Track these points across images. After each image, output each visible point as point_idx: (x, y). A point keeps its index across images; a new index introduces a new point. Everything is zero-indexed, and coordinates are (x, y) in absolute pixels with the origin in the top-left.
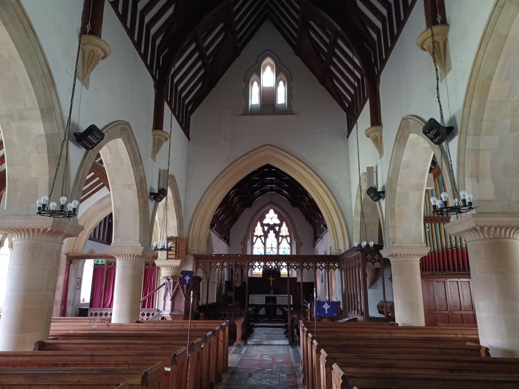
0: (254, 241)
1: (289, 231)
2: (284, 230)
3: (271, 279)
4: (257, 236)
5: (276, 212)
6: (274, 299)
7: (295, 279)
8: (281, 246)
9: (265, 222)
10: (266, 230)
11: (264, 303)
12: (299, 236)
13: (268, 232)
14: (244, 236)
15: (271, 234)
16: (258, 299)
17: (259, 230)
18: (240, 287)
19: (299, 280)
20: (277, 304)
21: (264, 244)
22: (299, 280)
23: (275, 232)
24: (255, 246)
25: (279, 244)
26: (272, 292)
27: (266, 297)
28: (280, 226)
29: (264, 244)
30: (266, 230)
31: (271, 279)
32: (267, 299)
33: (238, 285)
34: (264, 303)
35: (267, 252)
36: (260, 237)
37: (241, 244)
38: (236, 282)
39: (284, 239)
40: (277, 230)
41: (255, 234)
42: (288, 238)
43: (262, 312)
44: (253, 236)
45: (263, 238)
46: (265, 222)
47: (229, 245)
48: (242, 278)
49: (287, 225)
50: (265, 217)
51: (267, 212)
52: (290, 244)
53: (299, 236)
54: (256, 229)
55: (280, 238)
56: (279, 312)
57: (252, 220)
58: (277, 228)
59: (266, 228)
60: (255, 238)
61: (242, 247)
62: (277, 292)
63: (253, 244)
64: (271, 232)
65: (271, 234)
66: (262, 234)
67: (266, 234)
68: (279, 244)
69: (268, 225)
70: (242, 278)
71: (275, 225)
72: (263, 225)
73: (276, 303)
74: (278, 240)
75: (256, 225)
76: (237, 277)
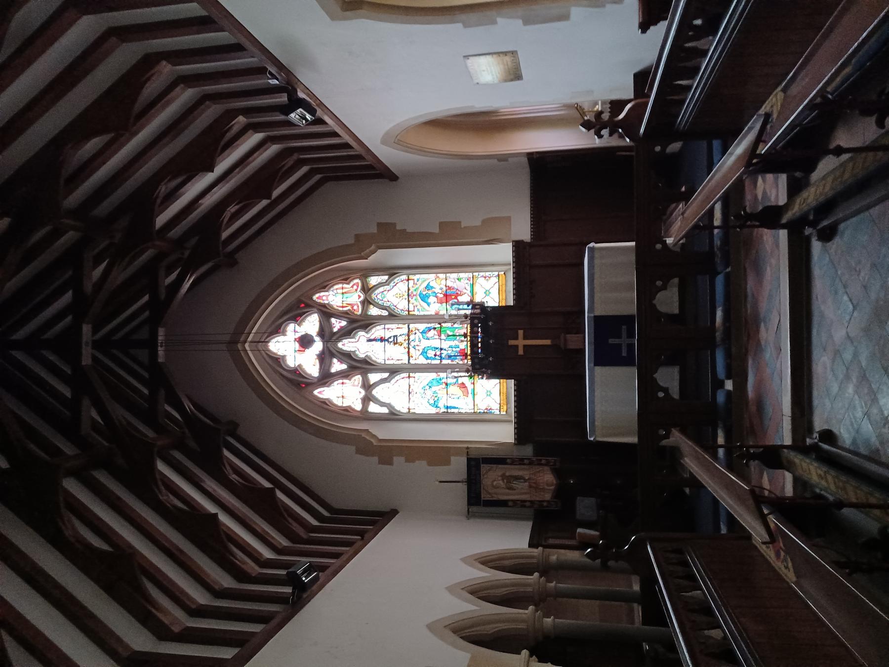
0: (385, 410)
1: (346, 280)
2: (342, 296)
3: (521, 342)
4: (367, 399)
5: (277, 330)
6: (606, 326)
7: (518, 246)
8: (401, 305)
9: (312, 369)
10: (344, 367)
11: (632, 373)
12: (357, 237)
13: (347, 356)
14: (359, 451)
15: (359, 345)
16: (611, 401)
17: (344, 394)
18: (557, 472)
19: (523, 230)
20: (633, 310)
21: (394, 371)
22: (525, 234)
23: (347, 333)
24: (401, 407)
25: (392, 316)
26: (572, 341)
27: (599, 361)
28: (326, 313)
29: (394, 371)
30: (344, 367)
31: (521, 342)
32: (606, 356)
33: (547, 478)
34: (632, 373)
35: (422, 361)
36: (368, 387)
37: (390, 463)
38: (535, 486)
39: (377, 295)
40: (344, 323)
41: (358, 406)
42: (373, 280)
43: (669, 378)
44: (365, 415)
45: (373, 377)
46: (312, 369)
47: (393, 513)
48: (521, 461)
49: (324, 287)
50: (297, 372)
51: (277, 361)
52: (392, 272)
53: (357, 237)
54: (338, 402)
55: (374, 311)
56: (668, 300)
57: (297, 421)
58: (337, 324)
59: (337, 366)
60: (373, 408)
61: (398, 460)
62: (573, 319)
63: (393, 416)
64: (346, 345)
65: (359, 345)
66: (358, 379)
67: (360, 366)
68: (392, 316)
69: (324, 358)
70: (521, 461)
71: (325, 333)
72: (326, 378)
73: (628, 320)
74: (379, 319)
75: (325, 403)
76: (516, 484)
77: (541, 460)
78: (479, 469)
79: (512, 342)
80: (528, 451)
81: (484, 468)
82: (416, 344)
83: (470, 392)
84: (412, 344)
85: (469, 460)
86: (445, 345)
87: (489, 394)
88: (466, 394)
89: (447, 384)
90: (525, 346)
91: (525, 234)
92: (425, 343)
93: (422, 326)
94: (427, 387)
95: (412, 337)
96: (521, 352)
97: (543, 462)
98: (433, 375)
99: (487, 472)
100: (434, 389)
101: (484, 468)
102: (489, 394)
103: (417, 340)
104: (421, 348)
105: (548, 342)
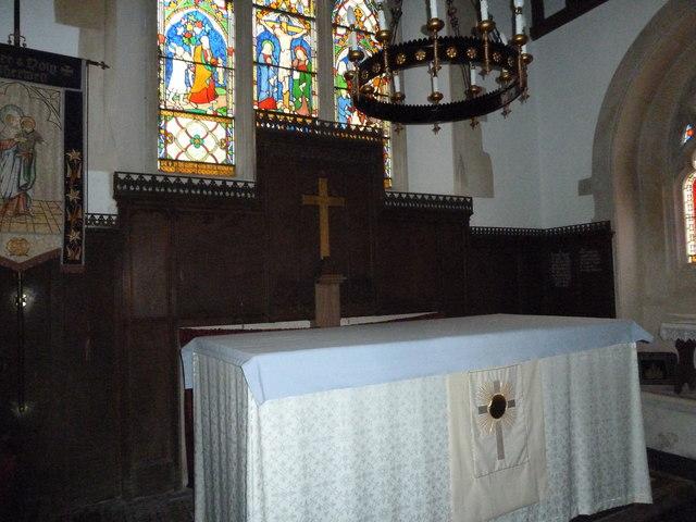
35: (257, 30)
77: (78, 229)
78: (53, 81)
79: (323, 185)
80: (100, 200)
81: (57, 95)
82: (284, 25)
83: (201, 106)
84: (284, 19)
85: (75, 64)
86: (283, 73)
87: (197, 141)
88: (196, 98)
89: (214, 65)
90: (317, 207)
91: (477, 220)
92: (285, 41)
93: (312, 40)
94: (208, 28)
95: (295, 21)
96: (306, 200)
97: (74, 236)
98: (231, 43)
99: (44, 99)
100: (205, 40)
101: (57, 95)
102: (197, 141)
103: (290, 29)
104: (278, 32)
105: (325, 251)
